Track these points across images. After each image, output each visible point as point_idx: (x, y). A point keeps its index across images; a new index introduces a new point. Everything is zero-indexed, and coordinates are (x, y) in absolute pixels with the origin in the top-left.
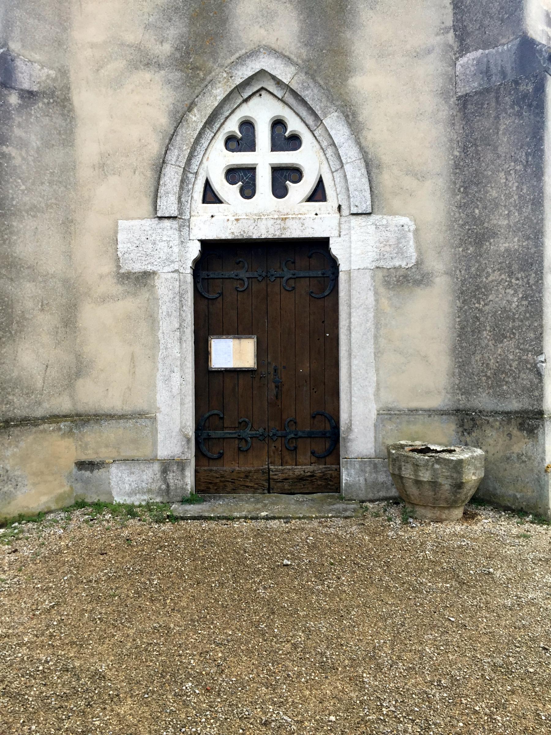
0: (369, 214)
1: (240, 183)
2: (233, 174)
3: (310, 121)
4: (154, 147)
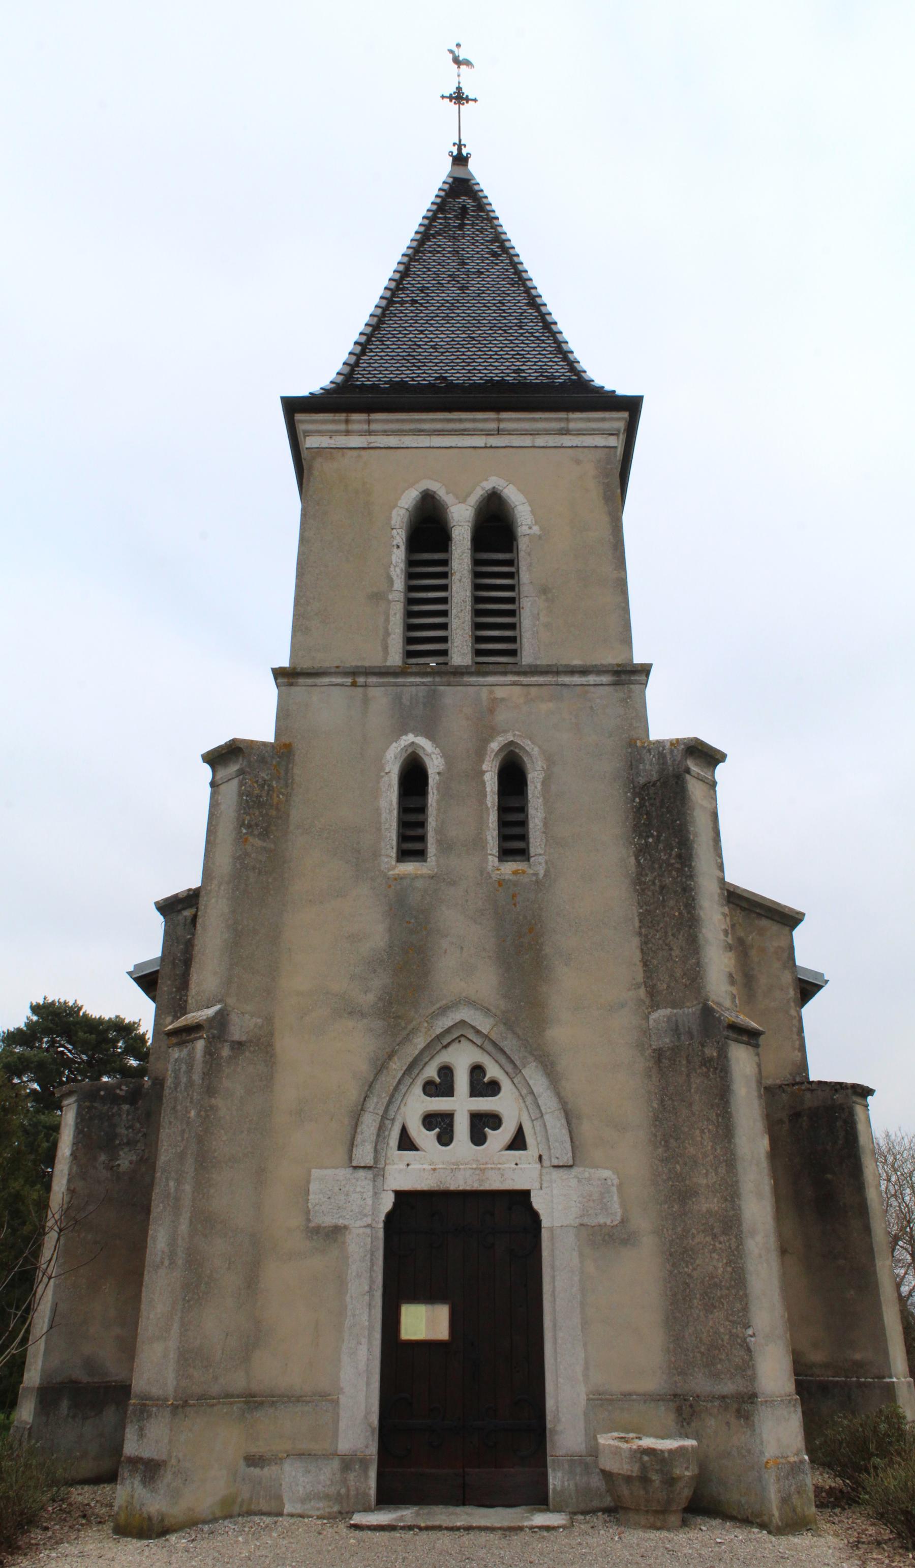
0: (571, 1166)
1: (437, 1130)
2: (430, 1120)
3: (509, 1068)
4: (353, 1094)
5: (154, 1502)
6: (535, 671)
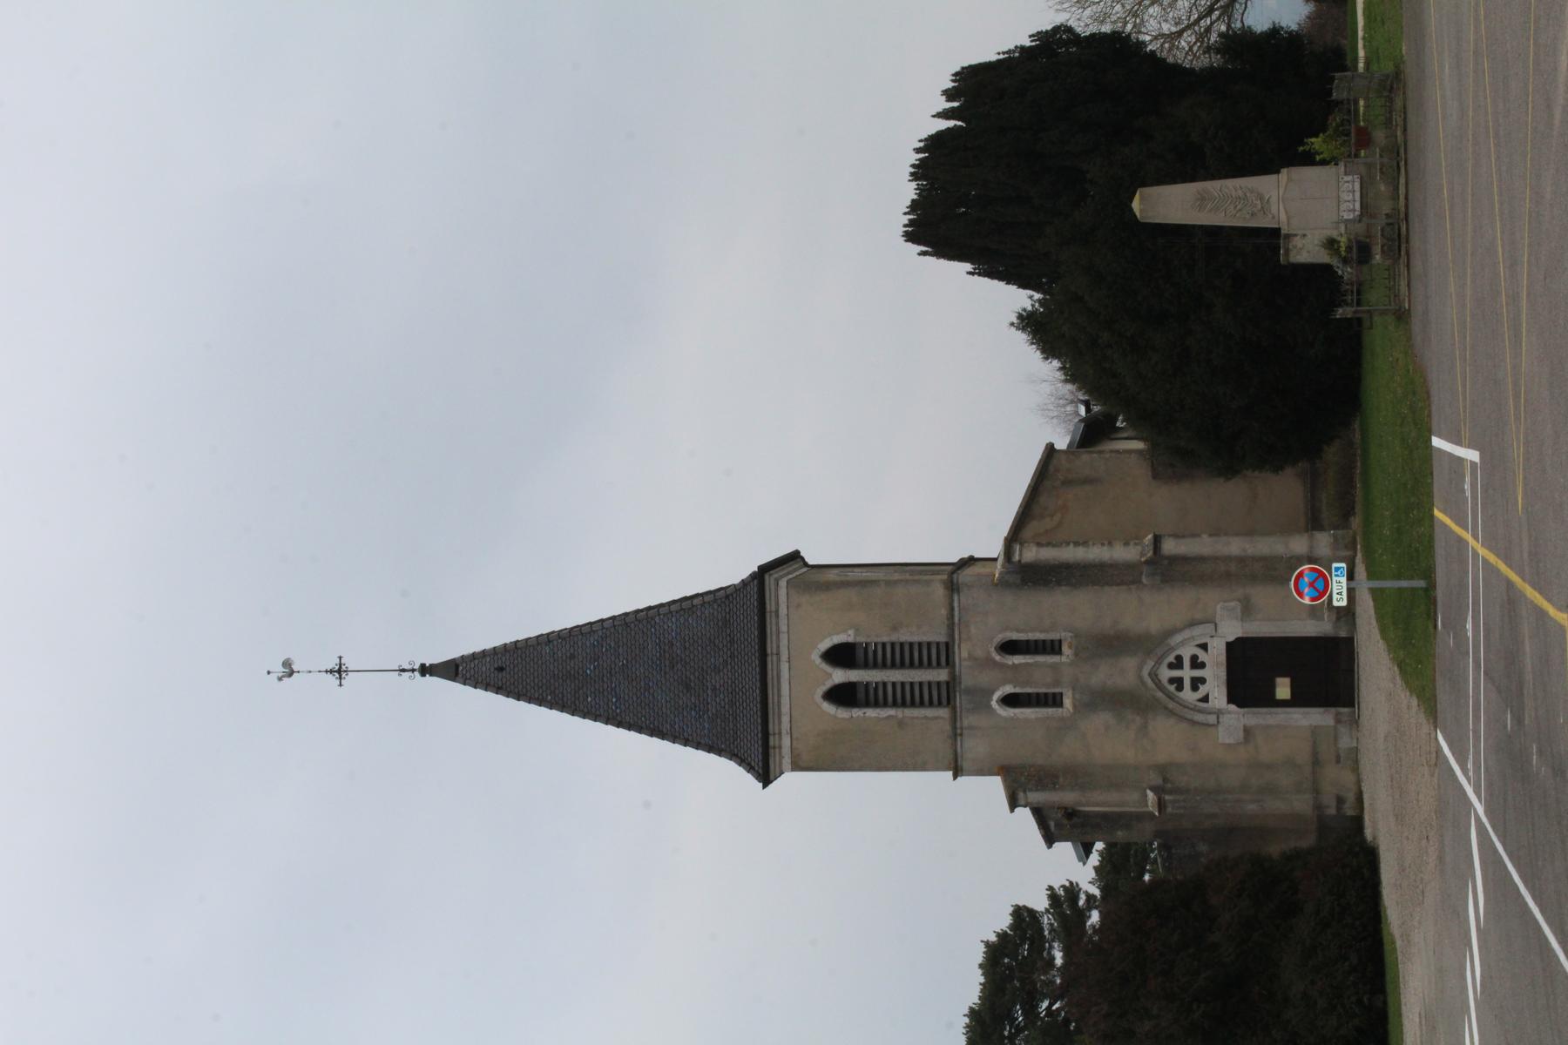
2: (1195, 688)
5: (1350, 797)
6: (952, 635)
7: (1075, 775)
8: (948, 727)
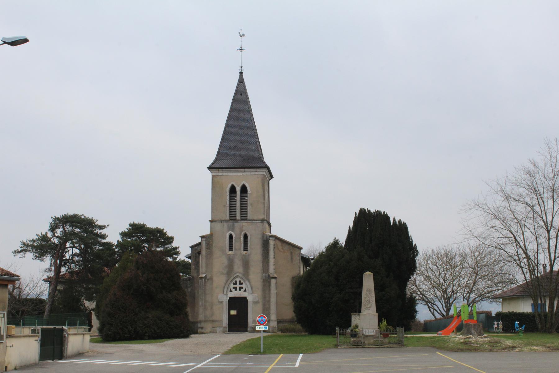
2: (234, 288)
5: (203, 331)
7: (210, 254)
8: (223, 219)
